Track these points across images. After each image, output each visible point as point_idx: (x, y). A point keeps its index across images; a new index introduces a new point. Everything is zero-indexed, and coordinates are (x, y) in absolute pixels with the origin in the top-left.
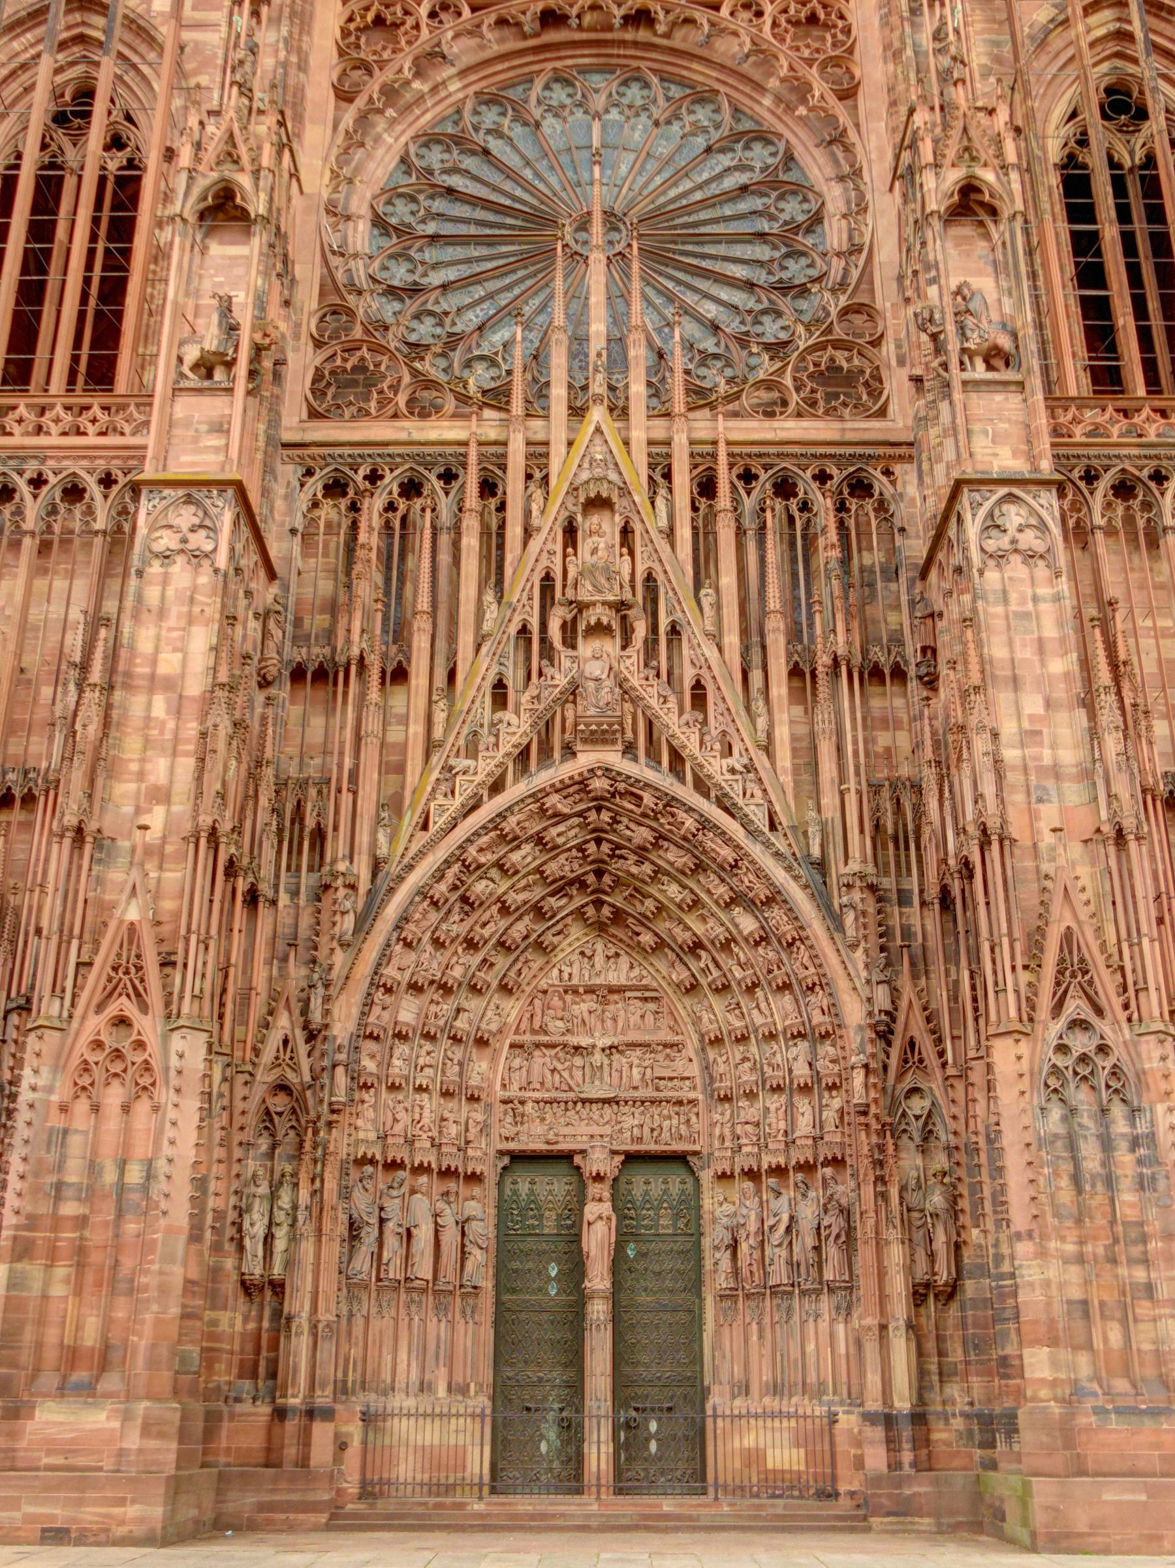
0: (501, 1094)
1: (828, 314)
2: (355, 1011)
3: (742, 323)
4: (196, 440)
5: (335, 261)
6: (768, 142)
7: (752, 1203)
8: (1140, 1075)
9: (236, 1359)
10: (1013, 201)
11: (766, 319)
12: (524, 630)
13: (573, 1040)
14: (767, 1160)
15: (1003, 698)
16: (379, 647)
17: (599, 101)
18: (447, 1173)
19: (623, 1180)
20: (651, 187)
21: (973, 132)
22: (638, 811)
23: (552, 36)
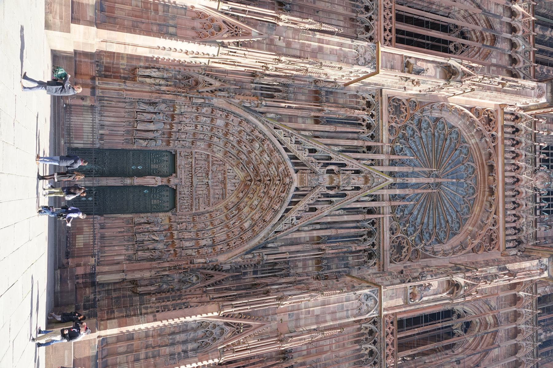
0: (194, 151)
1: (417, 245)
2: (221, 106)
3: (412, 221)
4: (389, 61)
5: (430, 105)
6: (459, 228)
8: (207, 352)
9: (111, 65)
10: (456, 299)
11: (413, 228)
12: (331, 158)
13: (210, 173)
14: (175, 233)
18: (170, 134)
19: (168, 189)
22: (280, 192)
23: (486, 168)
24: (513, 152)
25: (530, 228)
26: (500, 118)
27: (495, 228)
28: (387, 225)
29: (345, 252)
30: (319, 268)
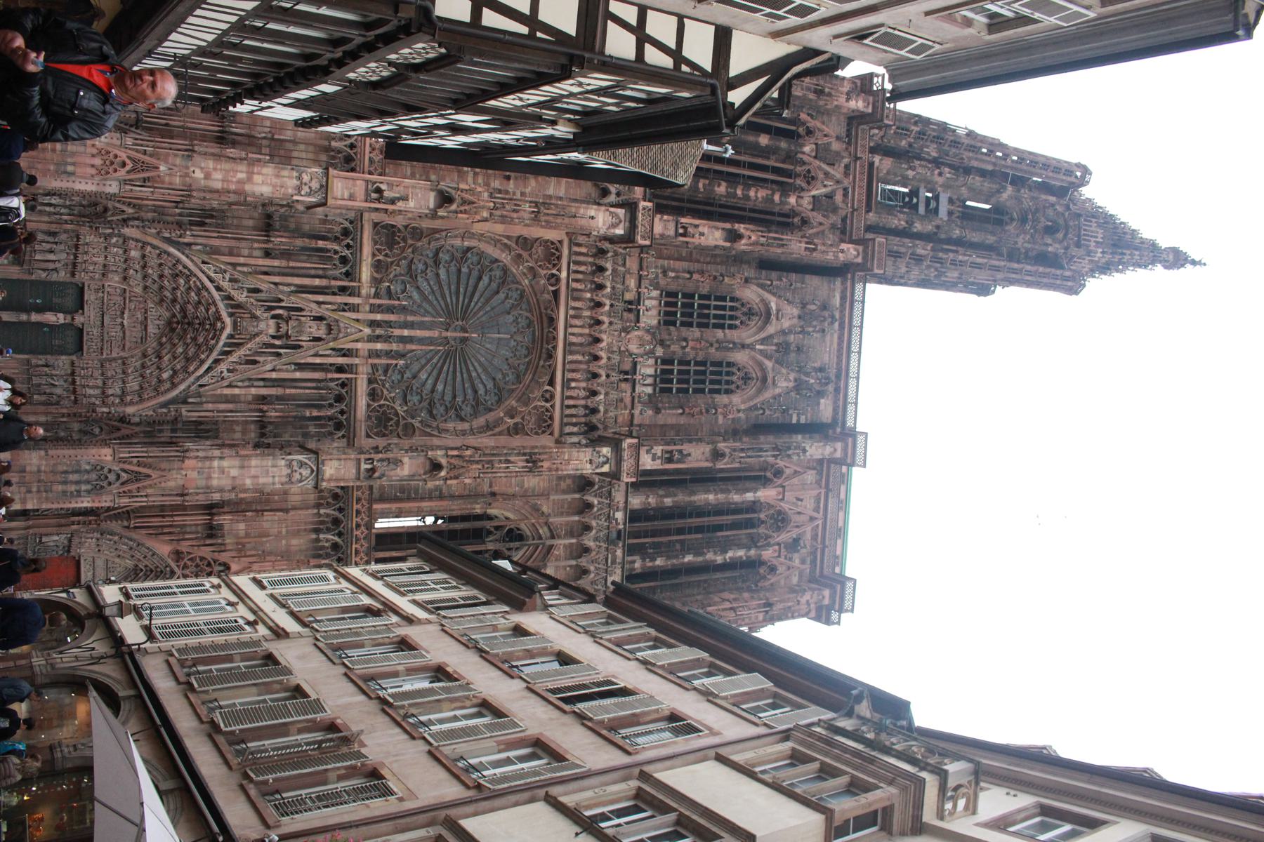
0: (106, 284)
1: (413, 418)
2: (134, 236)
7: (63, 372)
8: (101, 494)
11: (418, 397)
12: (280, 300)
13: (126, 312)
14: (78, 379)
15: (236, 462)
16: (277, 247)
17: (519, 338)
18: (74, 265)
20: (479, 356)
21: (461, 471)
23: (545, 319)
24: (592, 300)
25: (612, 409)
26: (565, 252)
27: (548, 405)
28: (362, 388)
29: (295, 417)
30: (263, 435)
